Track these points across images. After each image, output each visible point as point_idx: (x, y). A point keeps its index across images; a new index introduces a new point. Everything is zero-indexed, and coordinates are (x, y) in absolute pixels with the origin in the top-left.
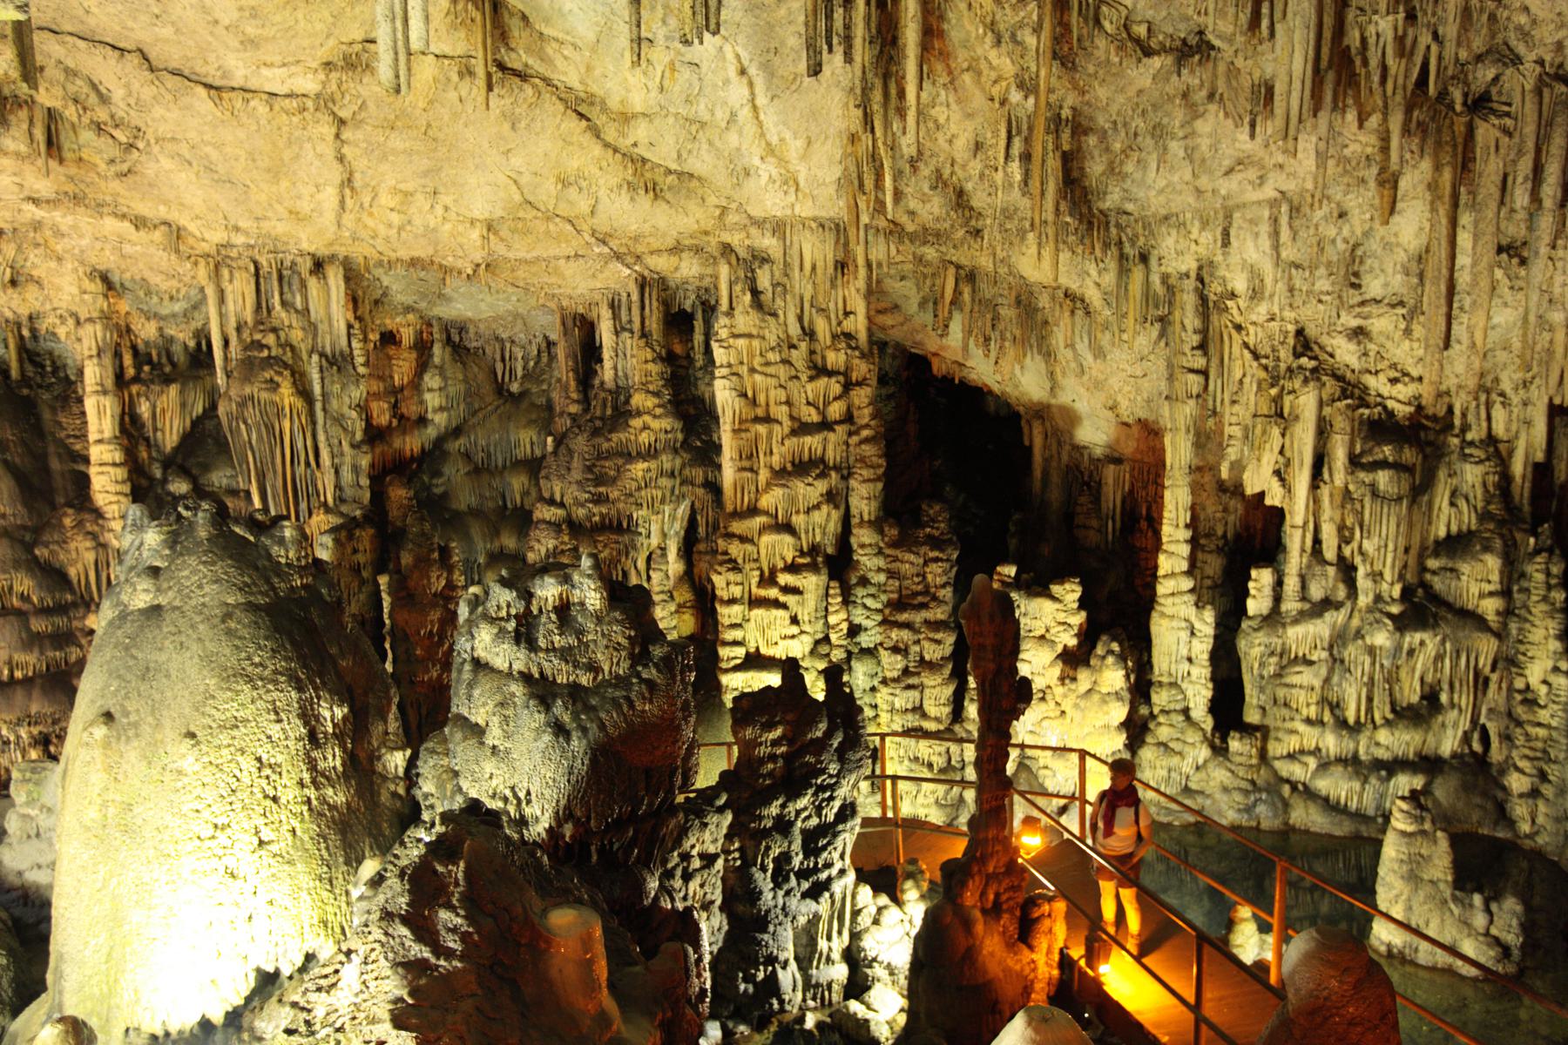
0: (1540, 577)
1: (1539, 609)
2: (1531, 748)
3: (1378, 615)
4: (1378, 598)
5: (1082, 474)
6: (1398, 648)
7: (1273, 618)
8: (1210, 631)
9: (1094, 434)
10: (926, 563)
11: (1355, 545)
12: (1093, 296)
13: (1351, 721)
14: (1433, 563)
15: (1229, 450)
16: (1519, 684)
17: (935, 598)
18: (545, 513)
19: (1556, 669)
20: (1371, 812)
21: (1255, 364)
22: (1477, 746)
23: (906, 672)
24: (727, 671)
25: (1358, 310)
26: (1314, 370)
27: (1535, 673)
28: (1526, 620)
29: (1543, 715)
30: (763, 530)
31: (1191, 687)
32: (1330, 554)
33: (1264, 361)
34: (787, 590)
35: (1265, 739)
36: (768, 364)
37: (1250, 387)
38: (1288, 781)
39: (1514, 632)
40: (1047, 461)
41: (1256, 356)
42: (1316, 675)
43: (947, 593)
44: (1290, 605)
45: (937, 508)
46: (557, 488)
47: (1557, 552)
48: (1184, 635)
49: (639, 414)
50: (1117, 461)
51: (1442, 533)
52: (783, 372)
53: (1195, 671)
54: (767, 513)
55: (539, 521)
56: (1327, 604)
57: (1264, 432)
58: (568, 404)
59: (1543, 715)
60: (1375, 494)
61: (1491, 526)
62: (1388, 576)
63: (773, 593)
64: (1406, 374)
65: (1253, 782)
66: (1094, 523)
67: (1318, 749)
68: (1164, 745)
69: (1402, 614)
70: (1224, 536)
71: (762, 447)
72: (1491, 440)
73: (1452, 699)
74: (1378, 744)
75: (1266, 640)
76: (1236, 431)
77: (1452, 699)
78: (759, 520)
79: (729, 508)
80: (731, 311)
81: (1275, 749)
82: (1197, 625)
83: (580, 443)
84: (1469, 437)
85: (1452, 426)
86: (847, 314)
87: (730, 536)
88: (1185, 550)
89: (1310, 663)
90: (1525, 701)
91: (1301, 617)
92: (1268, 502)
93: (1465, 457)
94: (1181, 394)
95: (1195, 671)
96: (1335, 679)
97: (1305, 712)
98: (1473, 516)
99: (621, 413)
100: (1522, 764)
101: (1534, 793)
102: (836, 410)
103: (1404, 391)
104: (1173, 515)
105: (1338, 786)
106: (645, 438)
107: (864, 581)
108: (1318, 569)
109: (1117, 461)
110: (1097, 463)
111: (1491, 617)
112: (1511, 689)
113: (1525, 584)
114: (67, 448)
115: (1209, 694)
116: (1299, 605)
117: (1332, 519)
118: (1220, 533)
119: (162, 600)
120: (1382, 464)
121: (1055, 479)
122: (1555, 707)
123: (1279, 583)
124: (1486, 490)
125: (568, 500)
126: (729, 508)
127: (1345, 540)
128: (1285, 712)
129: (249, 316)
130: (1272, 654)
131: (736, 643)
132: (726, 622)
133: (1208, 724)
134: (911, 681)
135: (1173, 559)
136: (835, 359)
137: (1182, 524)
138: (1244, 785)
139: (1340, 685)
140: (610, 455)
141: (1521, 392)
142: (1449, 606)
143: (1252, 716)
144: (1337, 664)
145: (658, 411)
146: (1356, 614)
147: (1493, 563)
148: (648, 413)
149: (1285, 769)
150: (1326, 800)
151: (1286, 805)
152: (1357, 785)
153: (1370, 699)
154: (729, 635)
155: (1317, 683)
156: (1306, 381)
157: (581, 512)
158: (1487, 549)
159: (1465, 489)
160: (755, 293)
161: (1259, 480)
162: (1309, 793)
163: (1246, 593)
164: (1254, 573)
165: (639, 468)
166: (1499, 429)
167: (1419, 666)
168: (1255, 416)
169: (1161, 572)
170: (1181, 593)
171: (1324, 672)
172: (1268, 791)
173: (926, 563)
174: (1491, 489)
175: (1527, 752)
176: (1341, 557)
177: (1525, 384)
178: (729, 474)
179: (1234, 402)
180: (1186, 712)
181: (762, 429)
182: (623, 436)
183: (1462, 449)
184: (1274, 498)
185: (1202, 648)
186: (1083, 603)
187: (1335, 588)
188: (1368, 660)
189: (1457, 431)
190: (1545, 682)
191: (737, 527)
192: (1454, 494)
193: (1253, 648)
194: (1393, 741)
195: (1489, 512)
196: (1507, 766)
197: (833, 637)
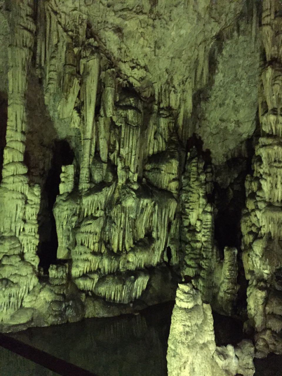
0: (194, 169)
2: (194, 254)
3: (128, 190)
4: (128, 181)
6: (138, 207)
7: (75, 194)
8: (37, 200)
11: (115, 153)
13: (115, 250)
14: (148, 167)
15: (50, 86)
16: (186, 223)
19: (204, 212)
20: (126, 302)
21: (65, 34)
22: (166, 259)
25: (120, 13)
26: (97, 48)
27: (193, 218)
28: (188, 191)
31: (25, 238)
32: (104, 157)
33: (70, 33)
35: (70, 268)
38: (83, 291)
39: (183, 198)
41: (66, 31)
42: (98, 225)
44: (84, 186)
47: (201, 156)
48: (20, 203)
51: (151, 152)
53: (28, 228)
57: (70, 80)
59: (199, 236)
61: (173, 147)
62: (132, 169)
64: (139, 65)
65: (63, 295)
67: (99, 269)
68: (7, 280)
69: (138, 189)
70: (43, 169)
72: (169, 108)
73: (157, 235)
74: (128, 262)
75: (71, 207)
76: (54, 75)
77: (157, 235)
81: (75, 272)
82: (29, 197)
84: (161, 106)
85: (155, 100)
88: (21, 147)
89: (95, 218)
90: (189, 231)
91: (91, 192)
93: (159, 115)
95: (28, 228)
96: (107, 227)
97: (92, 247)
98: (164, 143)
100: (189, 262)
101: (197, 277)
104: (13, 123)
105: (111, 290)
108: (98, 166)
111: (174, 192)
112: (182, 227)
113: (187, 175)
115: (37, 242)
116: (88, 185)
117: (105, 137)
118: (41, 167)
120: (130, 107)
122: (206, 231)
124: (170, 131)
127: (111, 151)
128: (82, 249)
130: (74, 215)
133: (36, 262)
137: (19, 130)
138: (58, 298)
139: (109, 230)
141: (182, 86)
142: (156, 188)
143: (61, 254)
144: (108, 220)
146: (117, 190)
149: (81, 283)
150: (104, 298)
151: (84, 307)
152: (119, 287)
153: (124, 238)
155: (98, 230)
156: (92, 53)
158: (173, 157)
162: (94, 296)
163: (59, 181)
164: (63, 169)
166: (173, 104)
167: (145, 218)
168: (65, 65)
169: (6, 162)
170: (20, 175)
171: (102, 223)
172: (73, 300)
174: (172, 130)
175: (192, 256)
176: (109, 160)
177: (183, 83)
180: (22, 255)
183: (159, 111)
185: (32, 212)
187: (107, 176)
188: (123, 216)
189: (156, 103)
190: (198, 220)
193: (63, 213)
194: (136, 260)
195: (172, 140)
196: (182, 264)
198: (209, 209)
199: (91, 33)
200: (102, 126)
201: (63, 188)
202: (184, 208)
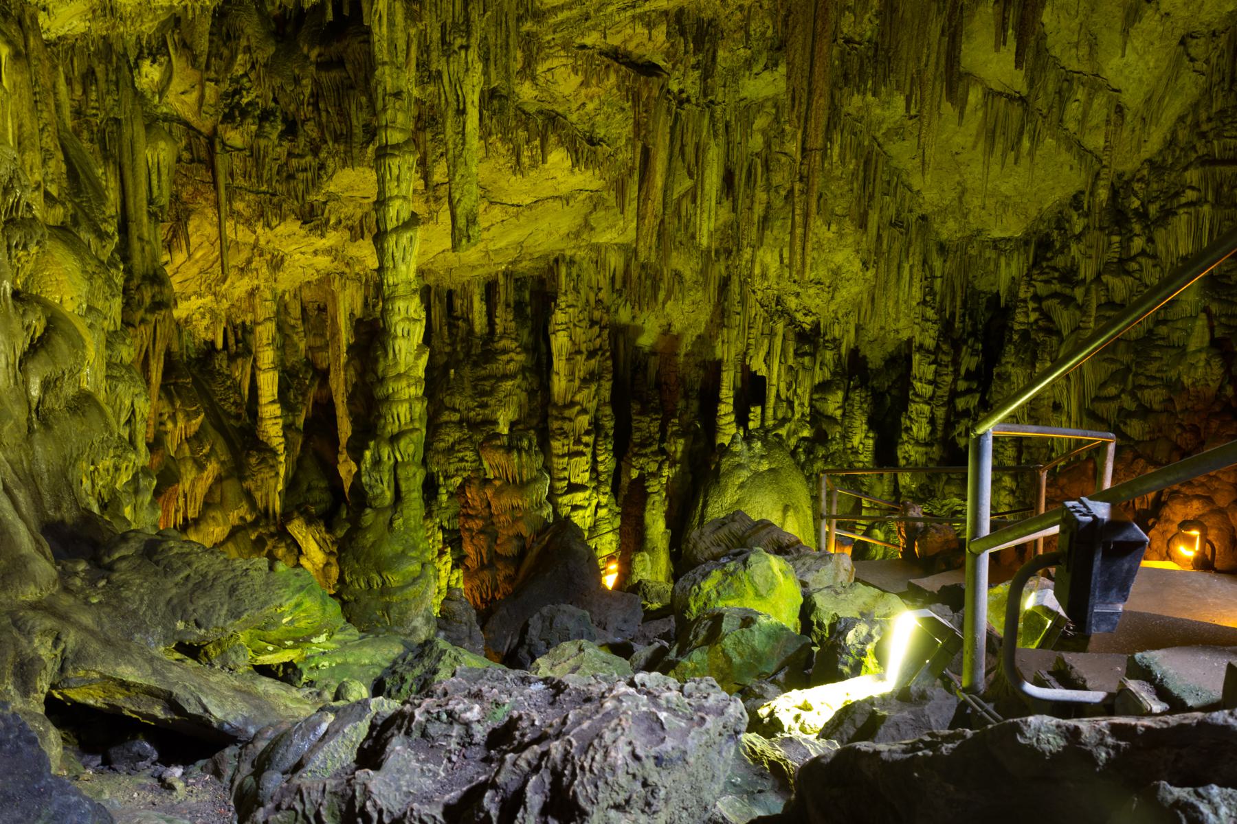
1: (858, 413)
4: (803, 415)
9: (646, 341)
12: (687, 274)
14: (815, 396)
16: (849, 446)
19: (866, 437)
24: (561, 495)
27: (856, 441)
29: (861, 457)
30: (579, 413)
32: (783, 397)
34: (587, 445)
37: (760, 321)
41: (762, 306)
43: (658, 436)
44: (770, 423)
46: (457, 401)
52: (583, 324)
55: (447, 423)
56: (784, 421)
59: (861, 457)
60: (804, 368)
63: (581, 448)
72: (834, 340)
78: (578, 408)
79: (561, 403)
80: (565, 294)
83: (467, 371)
86: (600, 289)
87: (564, 419)
88: (731, 401)
92: (759, 374)
99: (489, 355)
103: (809, 319)
106: (512, 366)
109: (653, 353)
110: (645, 354)
111: (839, 418)
119: (773, 466)
120: (804, 354)
125: (461, 408)
126: (561, 403)
131: (565, 479)
132: (560, 467)
135: (726, 408)
136: (597, 315)
142: (822, 414)
145: (518, 350)
147: (840, 394)
154: (562, 476)
157: (472, 414)
158: (838, 388)
161: (758, 366)
165: (508, 385)
166: (837, 334)
177: (847, 314)
178: (559, 385)
179: (750, 328)
184: (763, 372)
191: (567, 413)
192: (822, 364)
197: (601, 468)
198: (871, 435)
199: (779, 301)
201: (751, 425)
202: (847, 432)
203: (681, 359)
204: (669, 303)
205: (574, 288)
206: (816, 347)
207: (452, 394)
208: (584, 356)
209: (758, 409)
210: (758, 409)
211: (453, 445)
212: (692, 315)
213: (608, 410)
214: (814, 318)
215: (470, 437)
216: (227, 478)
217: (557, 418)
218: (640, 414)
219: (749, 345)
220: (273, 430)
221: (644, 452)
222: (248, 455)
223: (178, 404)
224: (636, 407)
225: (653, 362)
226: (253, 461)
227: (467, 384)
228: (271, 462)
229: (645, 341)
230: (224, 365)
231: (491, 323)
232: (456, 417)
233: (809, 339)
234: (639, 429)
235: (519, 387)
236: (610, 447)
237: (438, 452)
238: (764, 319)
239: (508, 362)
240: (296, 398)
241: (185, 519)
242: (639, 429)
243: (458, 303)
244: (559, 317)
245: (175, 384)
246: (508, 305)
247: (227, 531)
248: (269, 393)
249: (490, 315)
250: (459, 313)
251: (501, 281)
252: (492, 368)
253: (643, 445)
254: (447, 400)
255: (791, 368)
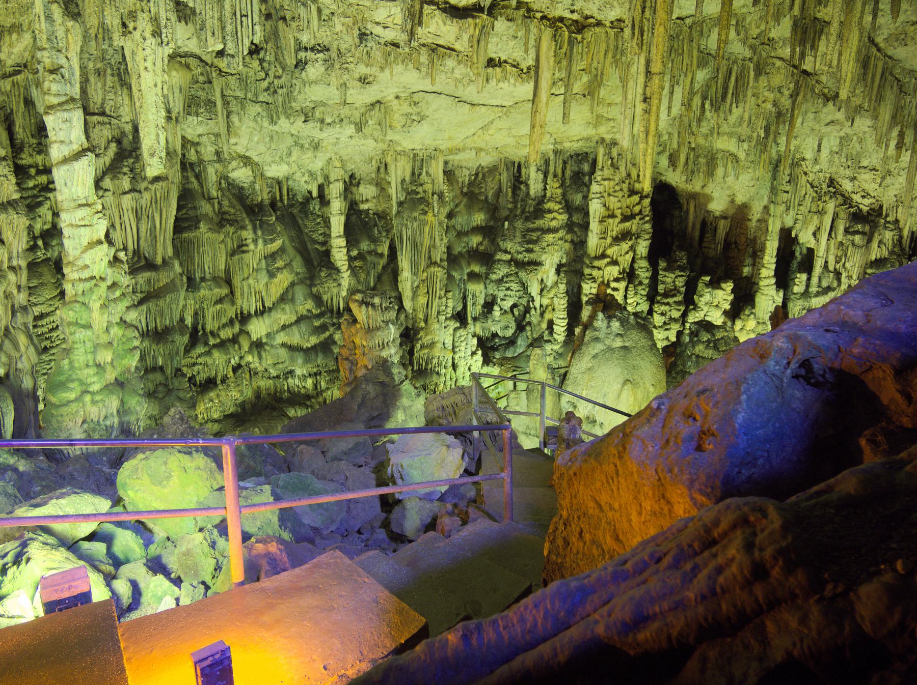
5: (707, 225)
9: (717, 206)
10: (676, 277)
11: (841, 264)
17: (679, 292)
18: (500, 256)
23: (665, 323)
30: (609, 264)
32: (831, 268)
34: (615, 289)
36: (615, 191)
37: (808, 200)
40: (696, 217)
41: (812, 187)
43: (683, 290)
44: (814, 289)
45: (683, 253)
46: (509, 245)
49: (550, 211)
50: (725, 218)
51: (873, 258)
52: (620, 194)
54: (609, 257)
55: (499, 260)
58: (506, 201)
60: (853, 245)
66: (713, 246)
71: (610, 228)
78: (608, 260)
80: (602, 170)
83: (519, 224)
85: (881, 214)
87: (594, 267)
88: (773, 266)
93: (886, 228)
94: (780, 202)
99: (539, 212)
102: (637, 209)
106: (554, 223)
107: (641, 283)
108: (826, 274)
109: (725, 218)
110: (716, 218)
114: (310, 237)
116: (817, 289)
120: (857, 232)
121: (698, 226)
123: (809, 279)
125: (512, 251)
126: (593, 255)
127: (837, 262)
129: (408, 179)
134: (667, 327)
140: (533, 230)
145: (561, 211)
148: (556, 211)
156: (831, 197)
159: (885, 241)
160: (612, 159)
161: (806, 238)
165: (550, 238)
169: (762, 276)
173: (676, 277)
176: (835, 269)
178: (593, 242)
181: (611, 220)
182: (541, 222)
184: (812, 244)
186: (733, 291)
191: (596, 263)
192: (880, 242)
200: (832, 246)
201: (796, 289)
203: (753, 224)
204: (730, 179)
205: (612, 165)
206: (874, 226)
207: (504, 240)
208: (617, 220)
209: (804, 277)
210: (804, 277)
211: (503, 277)
212: (753, 189)
213: (644, 264)
214: (873, 200)
215: (517, 273)
216: (298, 284)
217: (588, 267)
218: (665, 270)
219: (797, 219)
220: (340, 256)
221: (666, 301)
222: (320, 270)
223: (259, 233)
224: (662, 264)
225: (723, 227)
226: (323, 274)
227: (518, 234)
228: (334, 277)
229: (717, 206)
230: (317, 207)
231: (545, 189)
232: (508, 257)
233: (866, 220)
234: (663, 283)
235: (561, 239)
236: (644, 293)
237: (492, 281)
238: (813, 198)
239: (552, 220)
240: (380, 233)
241: (264, 306)
242: (663, 283)
243: (523, 170)
244: (595, 188)
245: (261, 220)
246: (555, 176)
247: (294, 318)
248: (337, 230)
249: (545, 182)
250: (523, 179)
251: (552, 158)
252: (539, 223)
253: (666, 295)
254: (501, 243)
255: (841, 244)
